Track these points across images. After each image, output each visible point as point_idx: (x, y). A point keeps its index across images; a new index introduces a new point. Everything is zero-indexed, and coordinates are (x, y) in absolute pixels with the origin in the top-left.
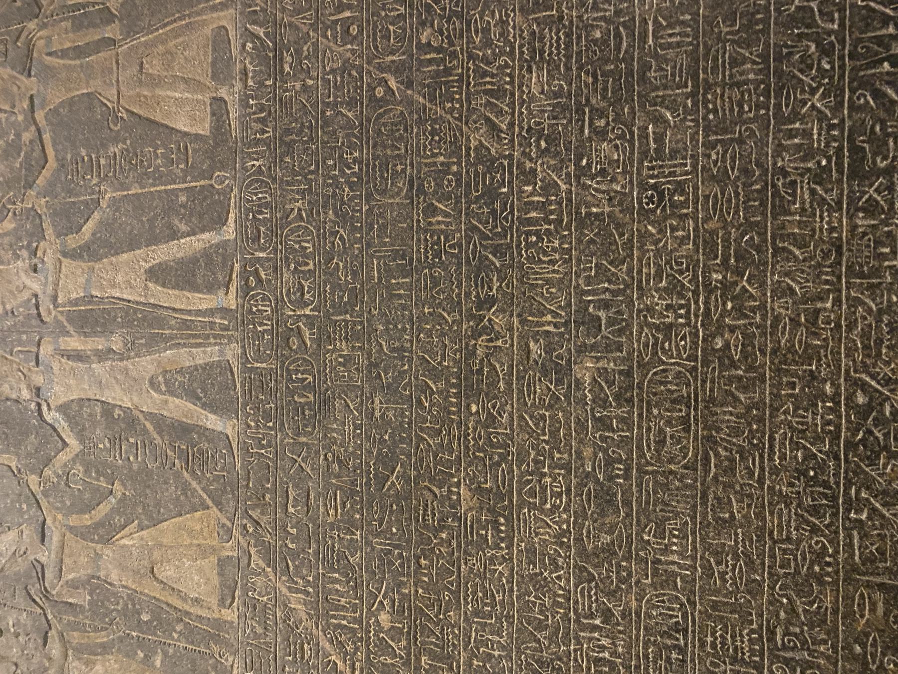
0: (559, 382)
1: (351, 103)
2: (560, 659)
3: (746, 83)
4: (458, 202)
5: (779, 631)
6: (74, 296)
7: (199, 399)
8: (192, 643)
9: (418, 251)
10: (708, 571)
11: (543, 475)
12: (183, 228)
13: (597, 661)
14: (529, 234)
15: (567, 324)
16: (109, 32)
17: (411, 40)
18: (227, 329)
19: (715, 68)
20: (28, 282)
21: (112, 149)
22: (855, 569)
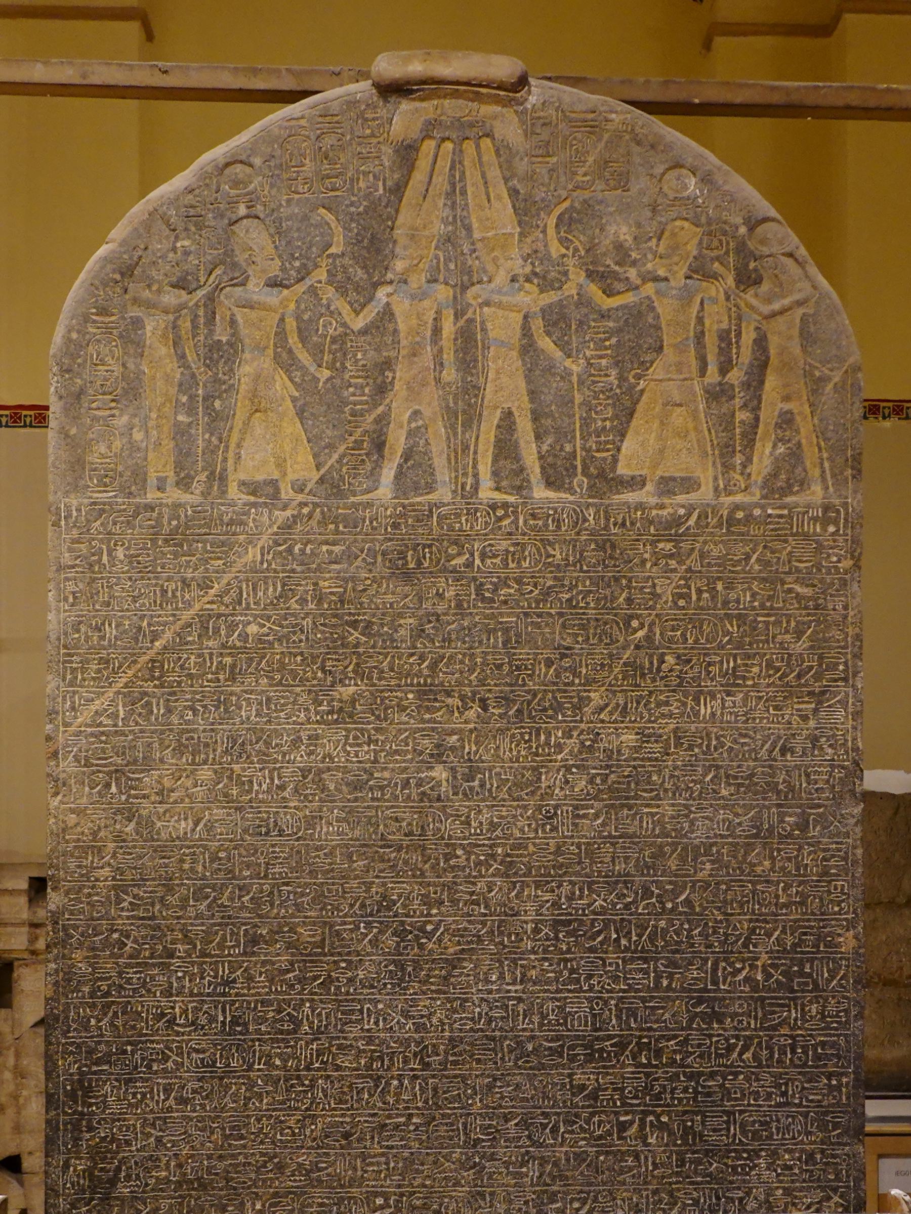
0: (432, 756)
1: (629, 601)
2: (248, 757)
3: (614, 865)
4: (555, 684)
5: (290, 888)
6: (489, 326)
7: (406, 461)
8: (204, 454)
9: (521, 654)
10: (317, 849)
11: (369, 745)
12: (545, 448)
13: (251, 782)
14: (530, 734)
15: (470, 760)
16: (712, 369)
17: (669, 648)
18: (463, 488)
19: (625, 848)
20: (502, 272)
21: (614, 372)
22: (331, 927)
